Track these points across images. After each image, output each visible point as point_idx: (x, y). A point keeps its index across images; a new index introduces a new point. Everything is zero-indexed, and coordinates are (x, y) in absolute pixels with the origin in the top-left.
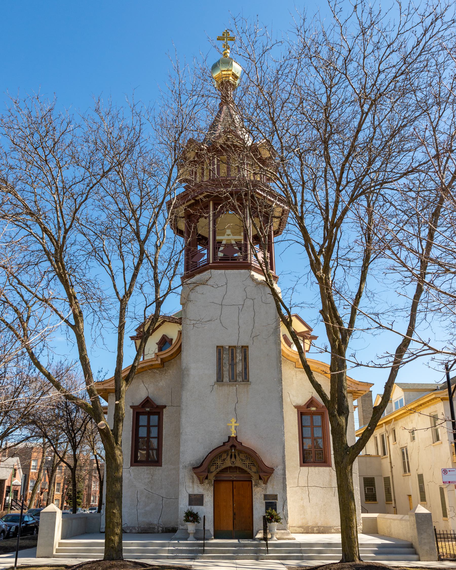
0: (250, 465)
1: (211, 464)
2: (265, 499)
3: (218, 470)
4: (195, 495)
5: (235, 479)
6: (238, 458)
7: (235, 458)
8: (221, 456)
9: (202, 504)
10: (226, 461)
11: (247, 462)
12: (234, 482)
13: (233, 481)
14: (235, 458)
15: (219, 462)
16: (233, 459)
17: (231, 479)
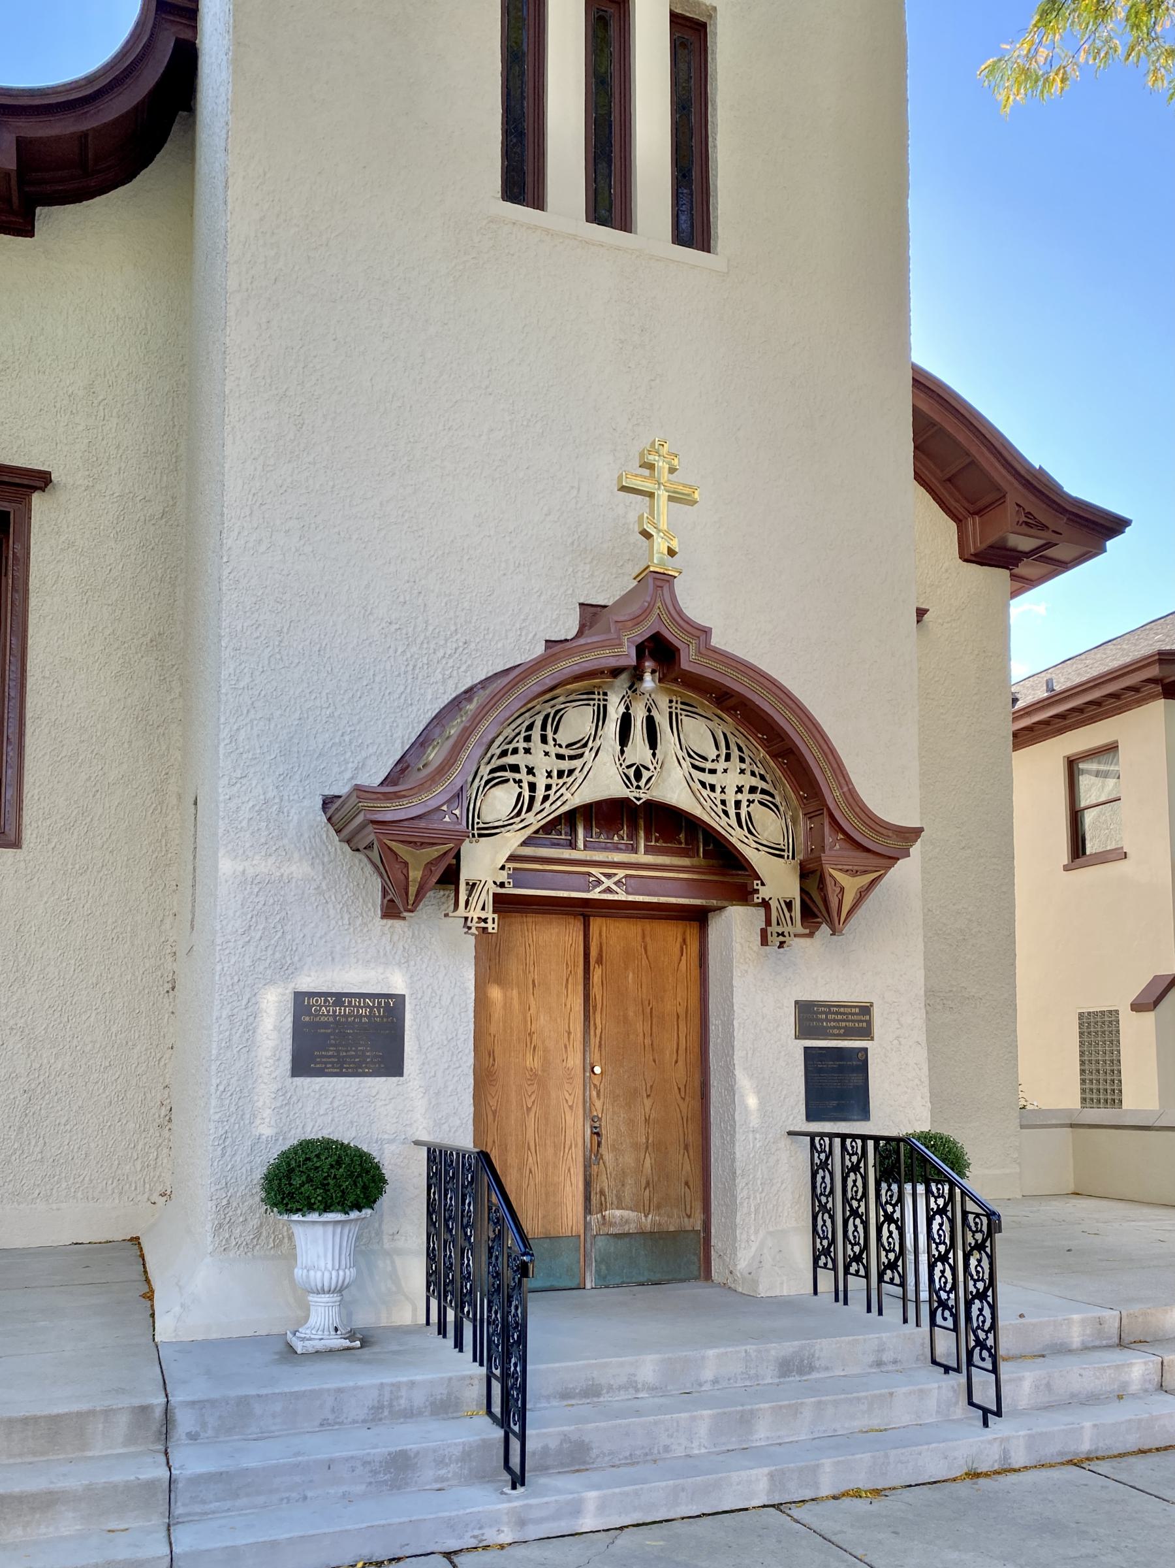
0: (744, 797)
1: (485, 771)
2: (803, 1031)
3: (530, 818)
4: (339, 998)
5: (622, 896)
6: (668, 740)
7: (653, 743)
8: (554, 721)
9: (392, 1065)
10: (588, 755)
11: (731, 778)
12: (596, 924)
13: (584, 911)
14: (653, 743)
15: (542, 760)
16: (639, 749)
17: (595, 894)
